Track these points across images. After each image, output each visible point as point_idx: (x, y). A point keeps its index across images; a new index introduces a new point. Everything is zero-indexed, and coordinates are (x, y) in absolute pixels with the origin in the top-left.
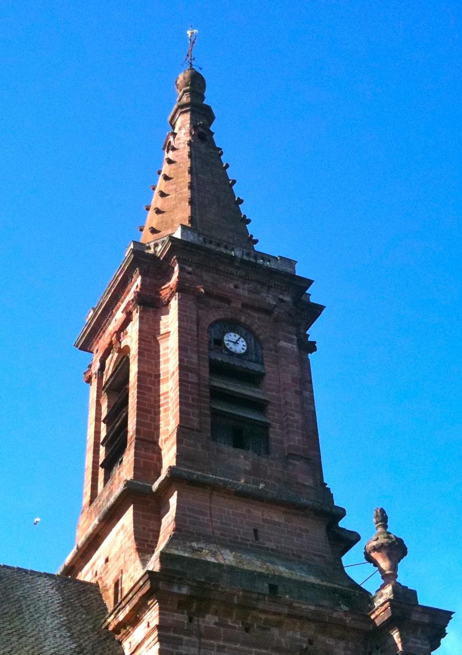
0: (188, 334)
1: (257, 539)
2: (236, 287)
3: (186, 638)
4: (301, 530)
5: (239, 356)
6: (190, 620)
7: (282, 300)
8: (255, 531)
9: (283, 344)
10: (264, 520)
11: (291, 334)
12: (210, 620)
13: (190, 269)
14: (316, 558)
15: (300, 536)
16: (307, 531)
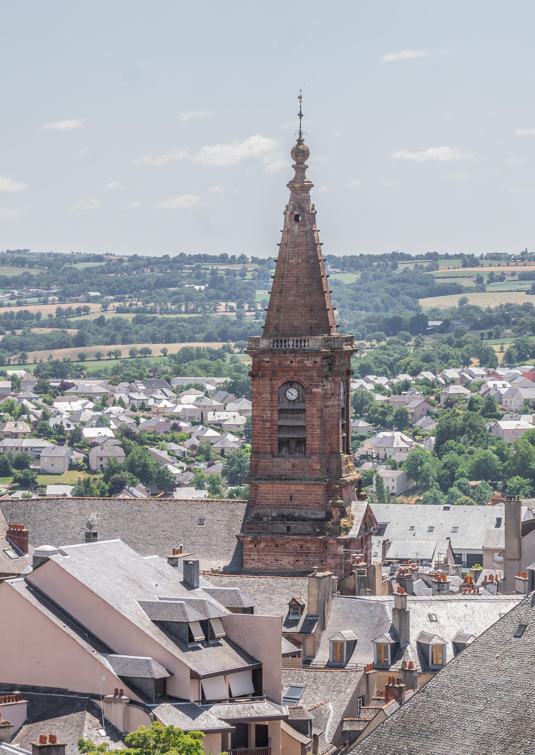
0: (266, 401)
1: (291, 500)
2: (291, 362)
3: (253, 553)
4: (312, 491)
5: (294, 401)
6: (255, 546)
7: (315, 362)
8: (291, 497)
9: (314, 390)
10: (296, 491)
11: (319, 382)
12: (262, 545)
13: (268, 360)
14: (315, 505)
15: (311, 494)
16: (315, 491)
